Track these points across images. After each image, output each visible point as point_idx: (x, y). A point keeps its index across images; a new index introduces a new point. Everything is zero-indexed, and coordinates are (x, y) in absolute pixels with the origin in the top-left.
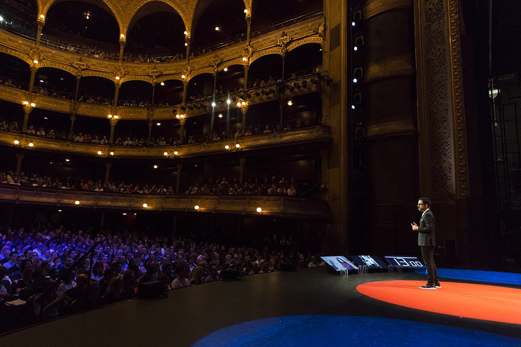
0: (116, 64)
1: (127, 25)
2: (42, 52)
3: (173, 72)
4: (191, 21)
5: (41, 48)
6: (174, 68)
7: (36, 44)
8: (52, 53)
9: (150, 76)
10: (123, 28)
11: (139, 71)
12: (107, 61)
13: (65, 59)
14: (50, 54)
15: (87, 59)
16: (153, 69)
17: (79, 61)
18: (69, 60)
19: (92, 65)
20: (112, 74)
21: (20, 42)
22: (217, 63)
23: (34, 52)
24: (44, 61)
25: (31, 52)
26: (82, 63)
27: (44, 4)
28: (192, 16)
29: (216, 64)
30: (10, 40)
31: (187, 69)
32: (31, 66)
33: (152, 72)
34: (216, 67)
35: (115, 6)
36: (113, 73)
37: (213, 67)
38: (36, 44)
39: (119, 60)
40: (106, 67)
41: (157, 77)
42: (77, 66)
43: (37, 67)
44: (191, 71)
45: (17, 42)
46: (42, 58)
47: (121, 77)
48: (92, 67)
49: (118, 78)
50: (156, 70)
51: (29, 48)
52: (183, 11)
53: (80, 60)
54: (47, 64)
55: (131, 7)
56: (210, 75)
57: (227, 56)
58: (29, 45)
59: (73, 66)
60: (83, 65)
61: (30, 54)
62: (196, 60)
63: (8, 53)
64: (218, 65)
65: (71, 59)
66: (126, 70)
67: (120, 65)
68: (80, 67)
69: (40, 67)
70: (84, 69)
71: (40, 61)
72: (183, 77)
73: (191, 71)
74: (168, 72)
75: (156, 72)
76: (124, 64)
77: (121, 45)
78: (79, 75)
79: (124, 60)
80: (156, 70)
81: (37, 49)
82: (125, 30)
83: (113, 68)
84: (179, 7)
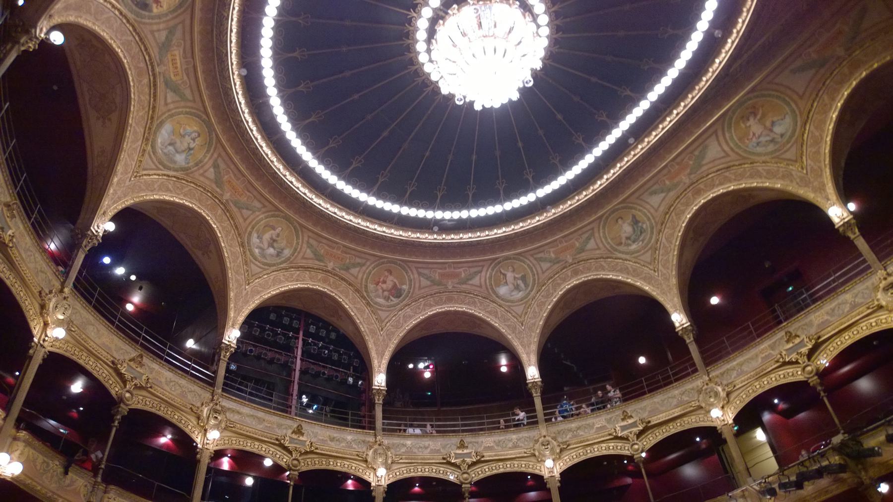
0: (533, 433)
1: (534, 347)
2: (388, 448)
3: (677, 412)
4: (675, 291)
5: (386, 441)
6: (675, 402)
7: (375, 436)
8: (404, 445)
9: (621, 438)
10: (528, 354)
11: (590, 435)
12: (514, 432)
13: (432, 451)
14: (403, 450)
15: (474, 440)
16: (623, 420)
17: (459, 448)
18: (438, 451)
19: (489, 448)
20: (533, 459)
21: (349, 438)
22: (805, 350)
23: (375, 451)
24: (395, 467)
25: (371, 453)
26: (465, 451)
27: (381, 355)
28: (674, 281)
29: (800, 354)
30: (332, 439)
31: (716, 394)
32: (373, 484)
33: (623, 428)
34: (803, 360)
35: (505, 320)
36: (535, 455)
37: (797, 362)
38: (375, 436)
39: (536, 423)
40: (515, 447)
41: (640, 434)
42: (458, 461)
43: (384, 483)
44: (728, 394)
45: (344, 440)
46: (390, 462)
47: (554, 460)
48: (488, 456)
49: (549, 463)
50: (630, 421)
51: (364, 449)
52: (648, 279)
53: (462, 446)
54: (402, 472)
55: (534, 312)
56: (803, 384)
57: (824, 325)
58: (364, 442)
59: (449, 463)
60: (469, 455)
61: (369, 460)
62: (728, 366)
63: (331, 467)
64: (811, 354)
65: (444, 448)
66: (560, 440)
67: (544, 433)
68: (464, 461)
69: (390, 482)
70: (474, 464)
71: (388, 468)
72: (716, 413)
73: (728, 394)
74: (662, 417)
75: (634, 425)
76: (554, 429)
77: (533, 391)
78: (466, 479)
79: (547, 421)
80: (630, 421)
81: (380, 445)
82: (534, 358)
83: (531, 445)
84: (636, 274)
